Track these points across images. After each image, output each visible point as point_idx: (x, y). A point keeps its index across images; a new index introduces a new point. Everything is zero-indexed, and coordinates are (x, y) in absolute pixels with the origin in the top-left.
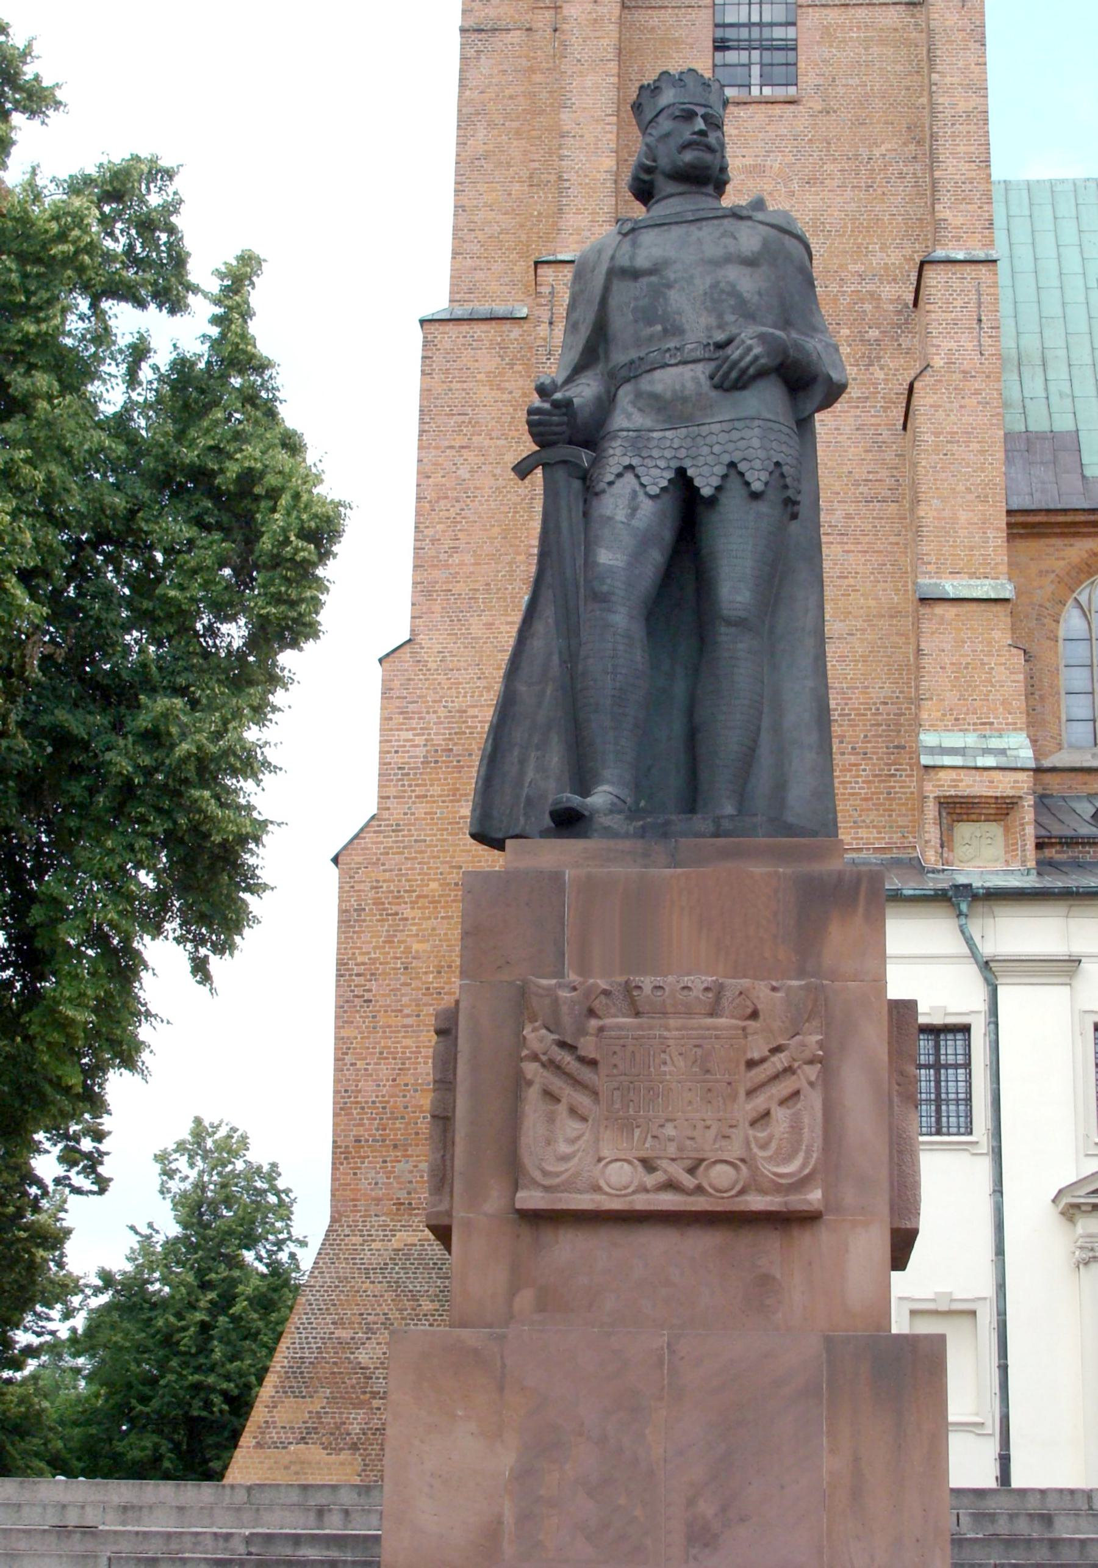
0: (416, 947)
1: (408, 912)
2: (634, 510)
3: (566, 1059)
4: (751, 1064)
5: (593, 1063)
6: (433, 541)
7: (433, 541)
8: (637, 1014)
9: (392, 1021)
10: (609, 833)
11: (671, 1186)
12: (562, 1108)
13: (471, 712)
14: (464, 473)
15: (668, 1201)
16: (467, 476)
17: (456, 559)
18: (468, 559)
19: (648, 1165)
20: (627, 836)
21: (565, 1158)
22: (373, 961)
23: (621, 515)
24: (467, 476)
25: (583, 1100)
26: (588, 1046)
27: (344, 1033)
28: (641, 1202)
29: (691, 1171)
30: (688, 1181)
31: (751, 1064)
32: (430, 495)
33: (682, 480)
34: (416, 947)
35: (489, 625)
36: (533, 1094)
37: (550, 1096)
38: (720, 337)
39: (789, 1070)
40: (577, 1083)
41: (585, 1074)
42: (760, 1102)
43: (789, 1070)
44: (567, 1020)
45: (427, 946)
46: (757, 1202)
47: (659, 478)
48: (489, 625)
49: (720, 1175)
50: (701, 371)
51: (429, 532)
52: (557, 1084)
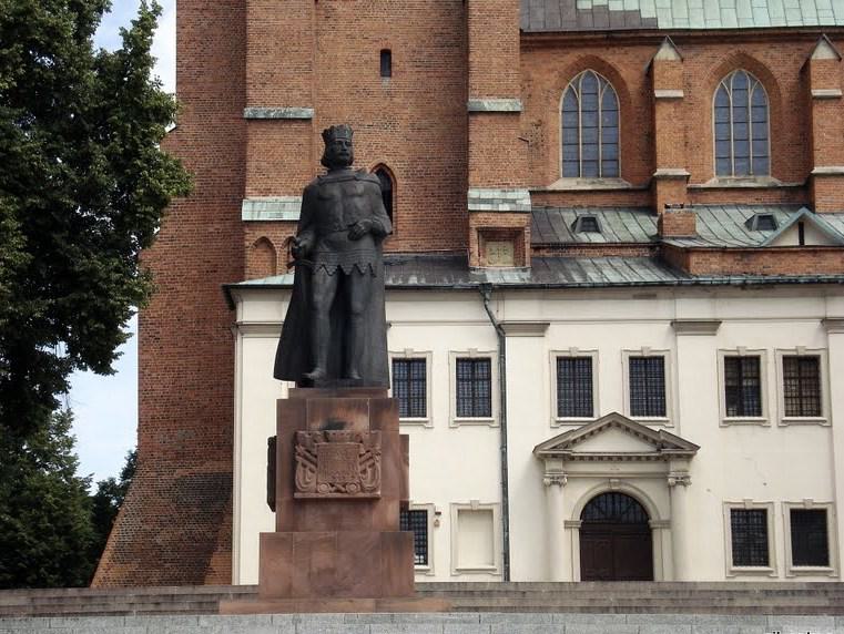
0: (184, 307)
1: (179, 288)
2: (324, 280)
3: (308, 454)
4: (360, 456)
5: (316, 457)
6: (188, 67)
7: (188, 67)
8: (328, 441)
9: (172, 350)
10: (319, 386)
11: (338, 491)
12: (307, 469)
13: (216, 171)
14: (204, 24)
15: (338, 495)
16: (206, 28)
17: (201, 79)
18: (209, 79)
19: (332, 486)
20: (325, 387)
21: (307, 483)
22: (160, 316)
23: (321, 282)
24: (206, 28)
25: (313, 467)
26: (315, 451)
27: (144, 357)
28: (330, 495)
29: (344, 486)
30: (343, 489)
31: (360, 456)
32: (185, 38)
33: (340, 270)
34: (184, 307)
35: (222, 120)
36: (299, 467)
37: (304, 466)
38: (351, 223)
39: (371, 458)
40: (312, 462)
41: (314, 459)
42: (363, 466)
43: (371, 458)
44: (308, 442)
45: (191, 307)
46: (361, 495)
47: (332, 269)
48: (222, 120)
49: (353, 488)
50: (345, 234)
51: (185, 62)
52: (306, 462)
